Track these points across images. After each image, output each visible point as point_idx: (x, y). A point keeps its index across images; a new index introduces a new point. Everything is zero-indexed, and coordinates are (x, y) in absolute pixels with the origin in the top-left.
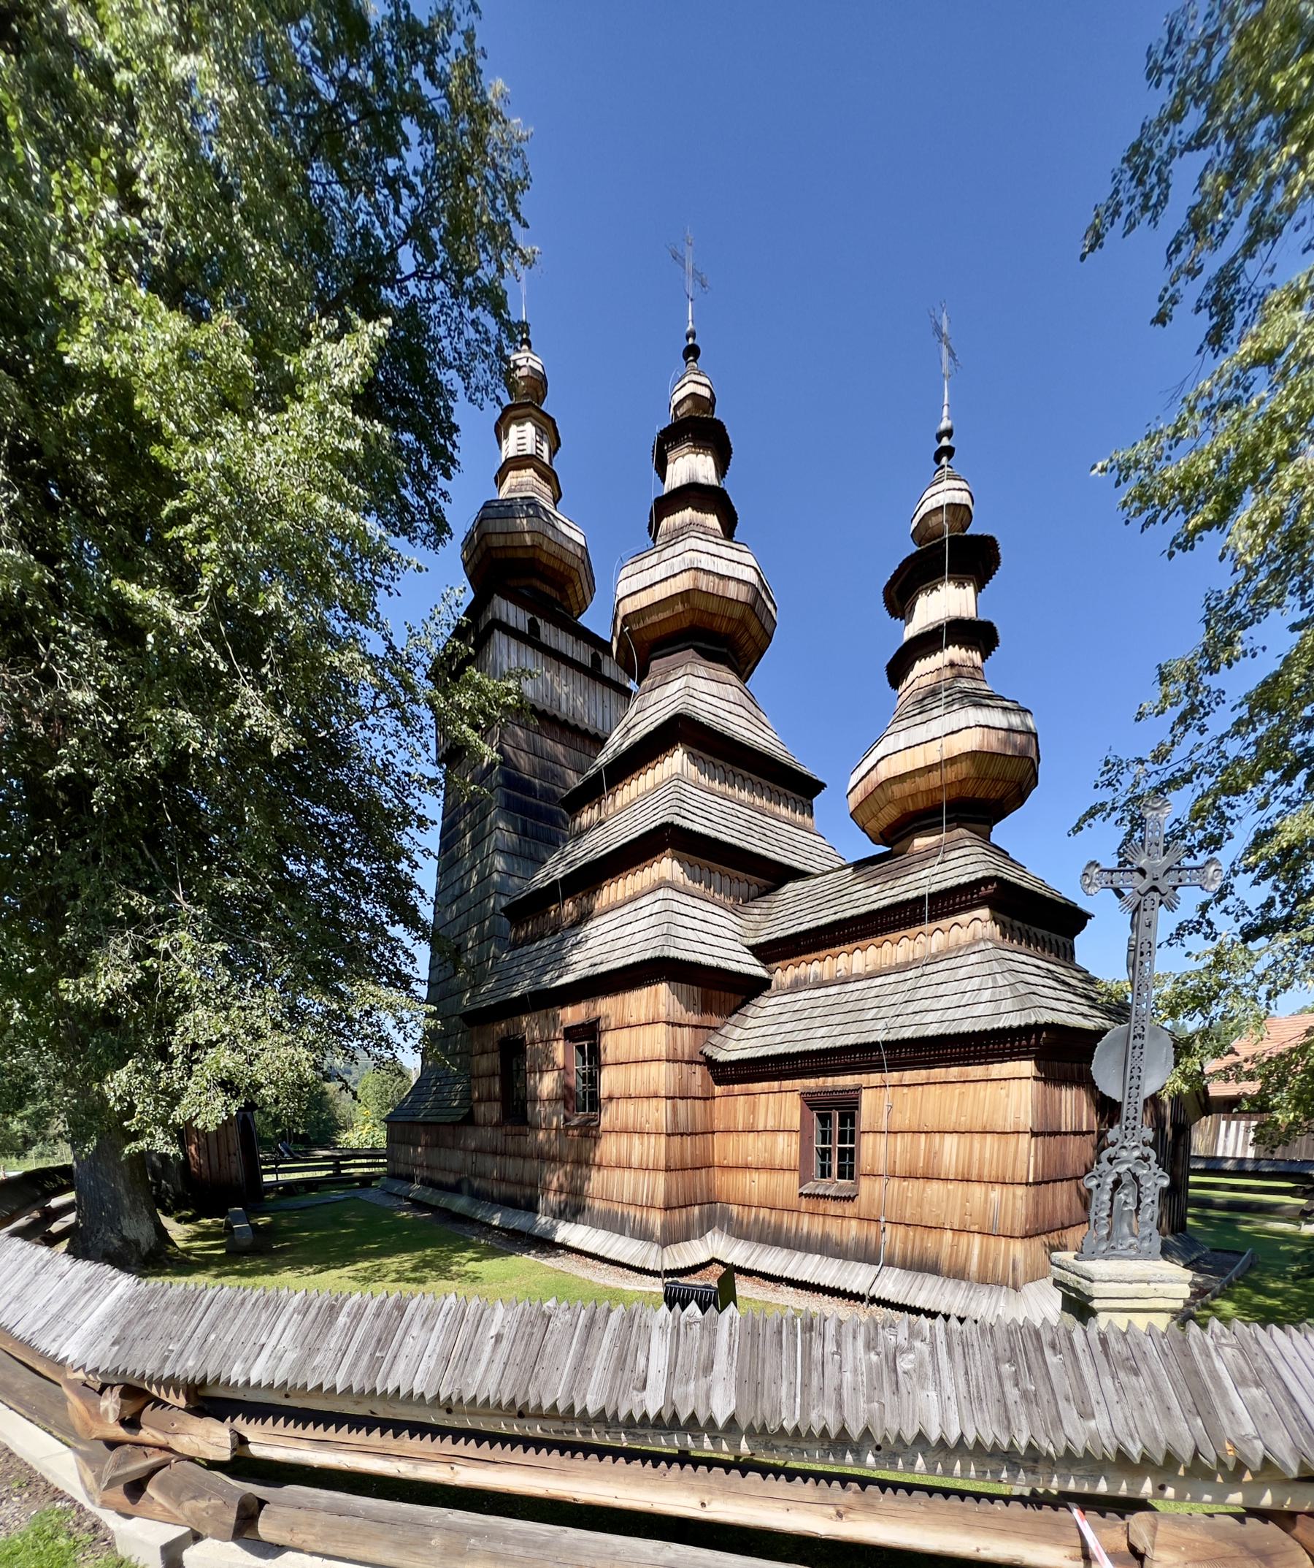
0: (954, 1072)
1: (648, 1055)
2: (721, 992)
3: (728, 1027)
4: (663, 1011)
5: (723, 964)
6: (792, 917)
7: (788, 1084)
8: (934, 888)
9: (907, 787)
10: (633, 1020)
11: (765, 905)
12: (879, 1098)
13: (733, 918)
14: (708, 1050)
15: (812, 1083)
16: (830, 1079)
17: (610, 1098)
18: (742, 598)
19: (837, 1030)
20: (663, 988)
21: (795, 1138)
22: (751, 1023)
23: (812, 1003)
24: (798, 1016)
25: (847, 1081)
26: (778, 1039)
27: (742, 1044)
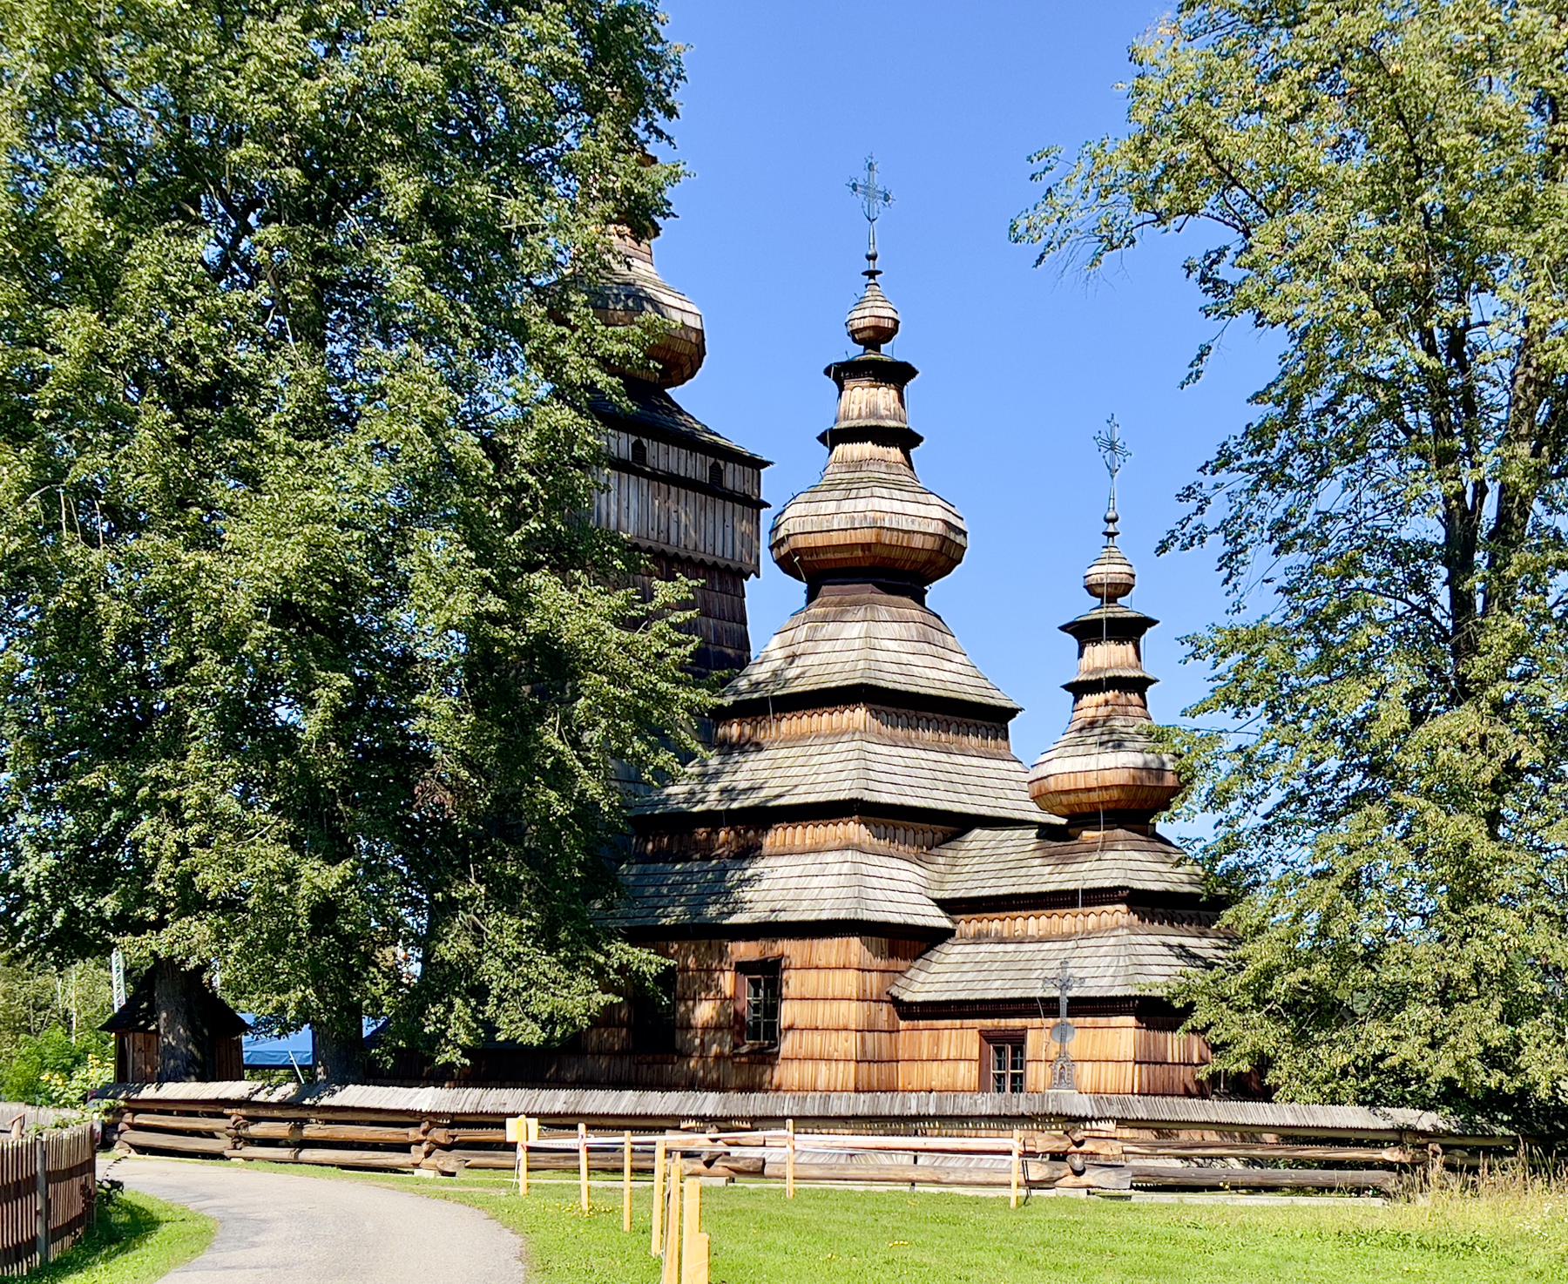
0: (1089, 1021)
1: (838, 994)
2: (906, 943)
3: (912, 971)
4: (854, 960)
5: (910, 921)
6: (976, 876)
7: (968, 1022)
8: (1088, 885)
9: (1072, 798)
10: (822, 963)
11: (950, 853)
12: (1039, 1036)
13: (918, 869)
14: (894, 991)
15: (989, 1023)
16: (1003, 1025)
18: (928, 546)
19: (1010, 984)
20: (855, 941)
21: (975, 1065)
22: (935, 968)
23: (991, 957)
24: (978, 967)
25: (1016, 1023)
26: (960, 986)
27: (927, 987)
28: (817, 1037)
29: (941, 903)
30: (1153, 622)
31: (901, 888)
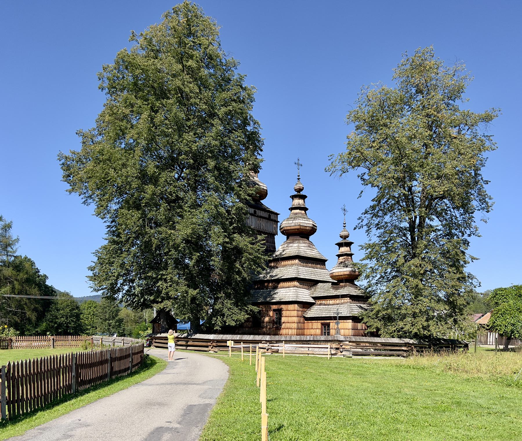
2: (306, 305)
12: (333, 324)
15: (323, 321)
16: (325, 322)
17: (284, 323)
20: (296, 305)
22: (312, 310)
25: (328, 321)
28: (289, 324)
29: (313, 298)
30: (353, 243)
31: (305, 295)
